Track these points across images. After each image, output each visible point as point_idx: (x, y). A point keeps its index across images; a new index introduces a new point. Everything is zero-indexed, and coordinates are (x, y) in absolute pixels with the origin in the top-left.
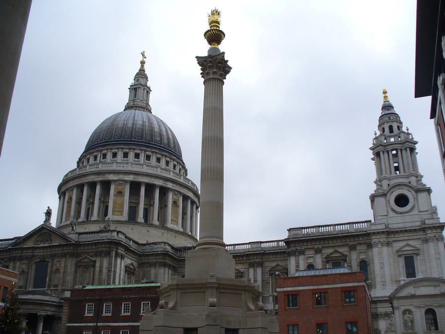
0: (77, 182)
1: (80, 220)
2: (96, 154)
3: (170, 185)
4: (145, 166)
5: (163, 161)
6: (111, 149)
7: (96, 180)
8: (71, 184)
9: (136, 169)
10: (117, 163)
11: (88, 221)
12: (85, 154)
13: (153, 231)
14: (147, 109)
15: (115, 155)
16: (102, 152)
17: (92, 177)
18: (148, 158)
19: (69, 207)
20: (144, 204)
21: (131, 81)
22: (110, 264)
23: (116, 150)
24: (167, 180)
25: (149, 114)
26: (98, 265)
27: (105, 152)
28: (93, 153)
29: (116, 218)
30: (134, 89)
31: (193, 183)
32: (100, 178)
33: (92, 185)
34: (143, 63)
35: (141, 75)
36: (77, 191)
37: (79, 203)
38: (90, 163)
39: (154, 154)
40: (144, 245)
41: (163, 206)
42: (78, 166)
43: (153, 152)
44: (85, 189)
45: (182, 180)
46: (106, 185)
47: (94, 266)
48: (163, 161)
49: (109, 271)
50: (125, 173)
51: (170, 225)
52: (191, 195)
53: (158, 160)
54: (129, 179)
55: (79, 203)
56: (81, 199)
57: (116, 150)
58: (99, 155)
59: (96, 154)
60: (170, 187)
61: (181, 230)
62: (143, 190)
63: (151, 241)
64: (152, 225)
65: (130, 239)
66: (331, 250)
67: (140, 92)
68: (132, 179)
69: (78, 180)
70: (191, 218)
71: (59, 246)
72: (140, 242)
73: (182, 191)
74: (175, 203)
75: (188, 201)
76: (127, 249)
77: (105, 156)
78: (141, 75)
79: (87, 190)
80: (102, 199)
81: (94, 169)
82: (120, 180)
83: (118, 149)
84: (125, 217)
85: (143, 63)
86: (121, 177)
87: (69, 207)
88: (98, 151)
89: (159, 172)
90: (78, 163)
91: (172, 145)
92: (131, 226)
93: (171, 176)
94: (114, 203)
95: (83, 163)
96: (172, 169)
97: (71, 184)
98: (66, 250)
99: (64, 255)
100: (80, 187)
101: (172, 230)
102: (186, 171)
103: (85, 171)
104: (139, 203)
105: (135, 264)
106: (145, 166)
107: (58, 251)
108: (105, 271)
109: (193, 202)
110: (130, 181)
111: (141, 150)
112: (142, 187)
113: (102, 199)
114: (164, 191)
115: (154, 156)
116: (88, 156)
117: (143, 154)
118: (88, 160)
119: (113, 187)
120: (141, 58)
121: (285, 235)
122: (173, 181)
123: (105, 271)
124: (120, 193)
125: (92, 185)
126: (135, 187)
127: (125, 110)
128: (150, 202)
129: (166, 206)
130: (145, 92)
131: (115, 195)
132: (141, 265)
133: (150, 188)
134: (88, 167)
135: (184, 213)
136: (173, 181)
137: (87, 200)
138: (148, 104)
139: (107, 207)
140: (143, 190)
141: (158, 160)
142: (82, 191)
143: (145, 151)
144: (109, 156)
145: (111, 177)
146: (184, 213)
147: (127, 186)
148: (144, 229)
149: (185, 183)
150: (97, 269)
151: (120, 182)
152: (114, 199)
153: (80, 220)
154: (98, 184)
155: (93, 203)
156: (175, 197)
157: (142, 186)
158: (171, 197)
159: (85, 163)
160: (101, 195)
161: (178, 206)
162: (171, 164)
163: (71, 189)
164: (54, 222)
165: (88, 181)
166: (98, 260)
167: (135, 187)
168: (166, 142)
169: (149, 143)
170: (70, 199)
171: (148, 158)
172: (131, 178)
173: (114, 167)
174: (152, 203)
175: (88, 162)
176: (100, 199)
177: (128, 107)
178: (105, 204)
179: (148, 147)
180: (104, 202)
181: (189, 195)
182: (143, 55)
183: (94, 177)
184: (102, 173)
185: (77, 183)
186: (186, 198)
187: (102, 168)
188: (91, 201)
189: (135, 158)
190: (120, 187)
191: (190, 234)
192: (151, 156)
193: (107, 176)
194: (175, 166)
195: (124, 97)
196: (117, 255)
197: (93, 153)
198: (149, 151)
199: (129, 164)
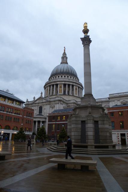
3: (74, 84)
5: (72, 78)
8: (47, 85)
9: (65, 80)
11: (52, 95)
13: (70, 97)
14: (67, 63)
15: (59, 77)
18: (68, 77)
19: (47, 92)
21: (62, 56)
25: (67, 65)
26: (56, 107)
29: (60, 94)
30: (63, 58)
31: (81, 83)
32: (55, 83)
33: (53, 85)
34: (65, 50)
35: (64, 54)
37: (50, 90)
40: (68, 101)
41: (73, 90)
45: (78, 82)
46: (57, 85)
48: (72, 78)
52: (80, 86)
53: (71, 77)
55: (50, 90)
62: (67, 86)
63: (70, 99)
64: (70, 95)
65: (64, 99)
66: (123, 100)
67: (65, 59)
70: (81, 93)
71: (45, 102)
72: (67, 100)
74: (76, 89)
76: (64, 102)
77: (56, 77)
78: (64, 54)
81: (54, 81)
85: (65, 50)
86: (61, 82)
87: (47, 92)
89: (71, 81)
91: (74, 73)
92: (64, 96)
93: (75, 81)
94: (59, 90)
97: (47, 85)
98: (47, 103)
99: (47, 105)
100: (50, 86)
102: (79, 80)
105: (66, 106)
107: (44, 103)
114: (73, 86)
118: (52, 78)
119: (59, 85)
120: (64, 49)
121: (108, 96)
122: (75, 83)
124: (61, 87)
125: (53, 85)
126: (65, 85)
129: (74, 90)
133: (69, 85)
135: (79, 92)
136: (75, 83)
138: (67, 62)
139: (57, 91)
140: (67, 86)
142: (50, 87)
144: (57, 77)
145: (58, 83)
148: (68, 97)
153: (50, 95)
155: (54, 90)
158: (75, 87)
160: (56, 88)
161: (77, 90)
162: (74, 78)
163: (47, 87)
164: (43, 96)
166: (56, 105)
168: (73, 72)
170: (47, 89)
172: (63, 83)
173: (59, 80)
177: (61, 63)
182: (64, 48)
186: (79, 87)
187: (55, 80)
194: (75, 79)
195: (60, 60)
196: (61, 104)
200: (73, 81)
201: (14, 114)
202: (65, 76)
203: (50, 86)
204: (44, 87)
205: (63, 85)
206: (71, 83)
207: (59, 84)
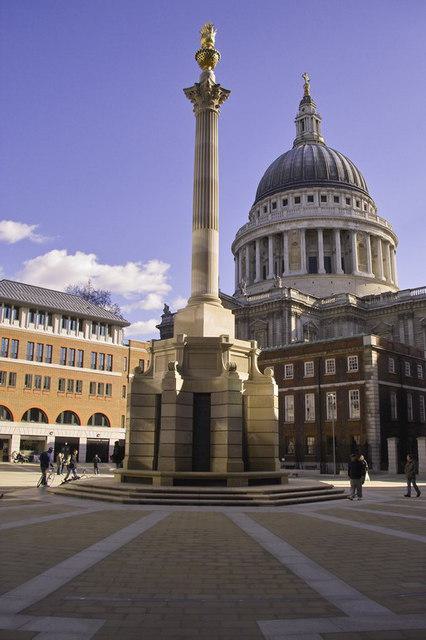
0: (249, 239)
1: (256, 281)
3: (352, 226)
8: (242, 243)
9: (311, 212)
15: (285, 202)
21: (296, 111)
22: (283, 325)
24: (347, 220)
30: (301, 122)
33: (265, 239)
44: (257, 245)
47: (267, 329)
49: (283, 334)
51: (358, 272)
53: (336, 199)
60: (353, 228)
61: (372, 276)
67: (307, 123)
78: (306, 100)
80: (278, 254)
84: (304, 270)
86: (294, 225)
87: (244, 268)
92: (312, 280)
94: (290, 256)
96: (355, 207)
101: (360, 278)
106: (319, 209)
108: (278, 333)
109: (386, 242)
113: (278, 254)
114: (346, 234)
119: (286, 238)
123: (278, 333)
124: (295, 244)
129: (351, 251)
130: (315, 122)
132: (322, 323)
133: (328, 233)
135: (375, 256)
141: (336, 199)
145: (282, 228)
146: (375, 256)
150: (271, 333)
156: (360, 239)
160: (275, 249)
161: (366, 249)
167: (311, 233)
171: (324, 199)
172: (305, 225)
176: (274, 254)
177: (296, 143)
179: (322, 186)
186: (374, 238)
191: (384, 279)
200: (346, 215)
201: (89, 370)
202: (311, 199)
203: (253, 243)
204: (233, 250)
206: (340, 225)
207: (288, 231)
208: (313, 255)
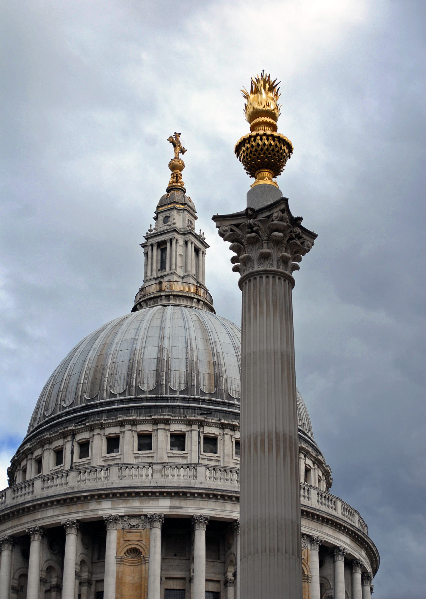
2: (59, 443)
4: (201, 470)
6: (102, 427)
7: (63, 519)
10: (121, 467)
12: (28, 446)
16: (79, 437)
17: (50, 512)
20: (207, 580)
23: (116, 430)
27: (85, 436)
28: (50, 441)
36: (11, 557)
38: (45, 471)
39: (227, 431)
42: (12, 481)
43: (223, 426)
50: (146, 494)
54: (158, 511)
56: (24, 576)
57: (116, 430)
58: (69, 446)
59: (59, 443)
68: (166, 511)
69: (9, 524)
73: (315, 534)
75: (334, 562)
79: (41, 549)
80: (85, 575)
82: (131, 517)
83: (121, 424)
88: (64, 436)
90: (11, 473)
95: (25, 471)
103: (29, 498)
104: (191, 580)
106: (201, 470)
110: (160, 516)
111: (190, 423)
112: (197, 533)
113: (85, 575)
115: (227, 437)
116: (38, 452)
117: (195, 435)
118: (39, 461)
127: (135, 309)
128: (225, 573)
131: (120, 561)
134: (38, 484)
137: (42, 581)
143: (202, 424)
147: (154, 530)
149: (324, 508)
151: (134, 522)
152: (118, 572)
154: (68, 531)
157: (197, 526)
159: (31, 473)
165: (40, 523)
169: (210, 402)
174: (230, 575)
175: (39, 470)
176: (78, 575)
178: (93, 587)
179: (209, 412)
180: (89, 583)
181: (338, 543)
183: (57, 512)
184: (78, 498)
185: (9, 533)
188: (54, 581)
189: (173, 445)
190: (133, 536)
192: (219, 438)
193: (93, 506)
197: (50, 443)
198: (211, 425)
199: (156, 467)
205: (157, 532)
207: (116, 519)
208: (174, 585)
